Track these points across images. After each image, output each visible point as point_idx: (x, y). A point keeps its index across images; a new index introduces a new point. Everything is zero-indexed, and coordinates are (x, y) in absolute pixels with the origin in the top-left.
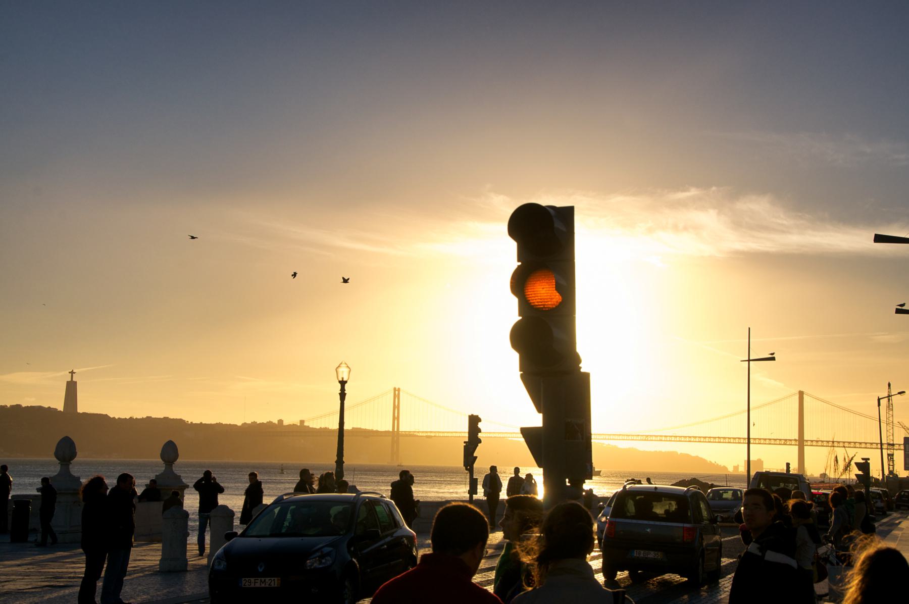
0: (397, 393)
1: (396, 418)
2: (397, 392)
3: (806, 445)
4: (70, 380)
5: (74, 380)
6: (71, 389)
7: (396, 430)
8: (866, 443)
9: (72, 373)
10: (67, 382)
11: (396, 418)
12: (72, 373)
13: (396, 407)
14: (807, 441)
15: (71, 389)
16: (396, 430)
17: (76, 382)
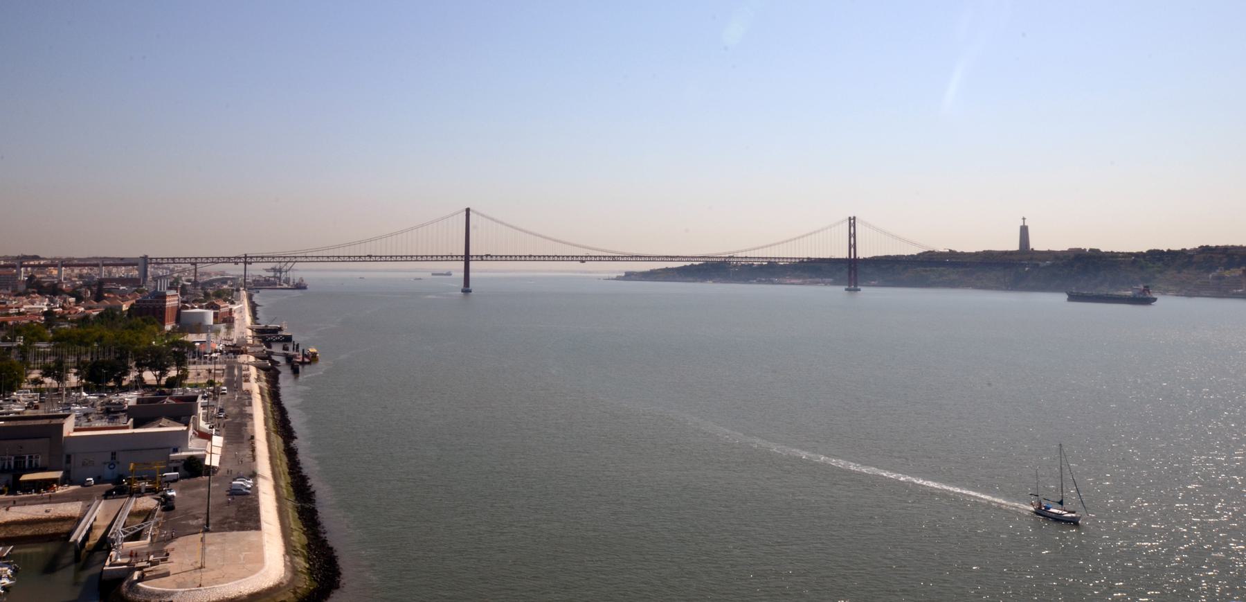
0: (852, 222)
1: (852, 246)
2: (852, 221)
6: (1024, 231)
7: (852, 257)
8: (427, 256)
9: (1024, 219)
11: (852, 246)
12: (1024, 219)
13: (852, 235)
14: (472, 256)
15: (1024, 231)
16: (852, 257)
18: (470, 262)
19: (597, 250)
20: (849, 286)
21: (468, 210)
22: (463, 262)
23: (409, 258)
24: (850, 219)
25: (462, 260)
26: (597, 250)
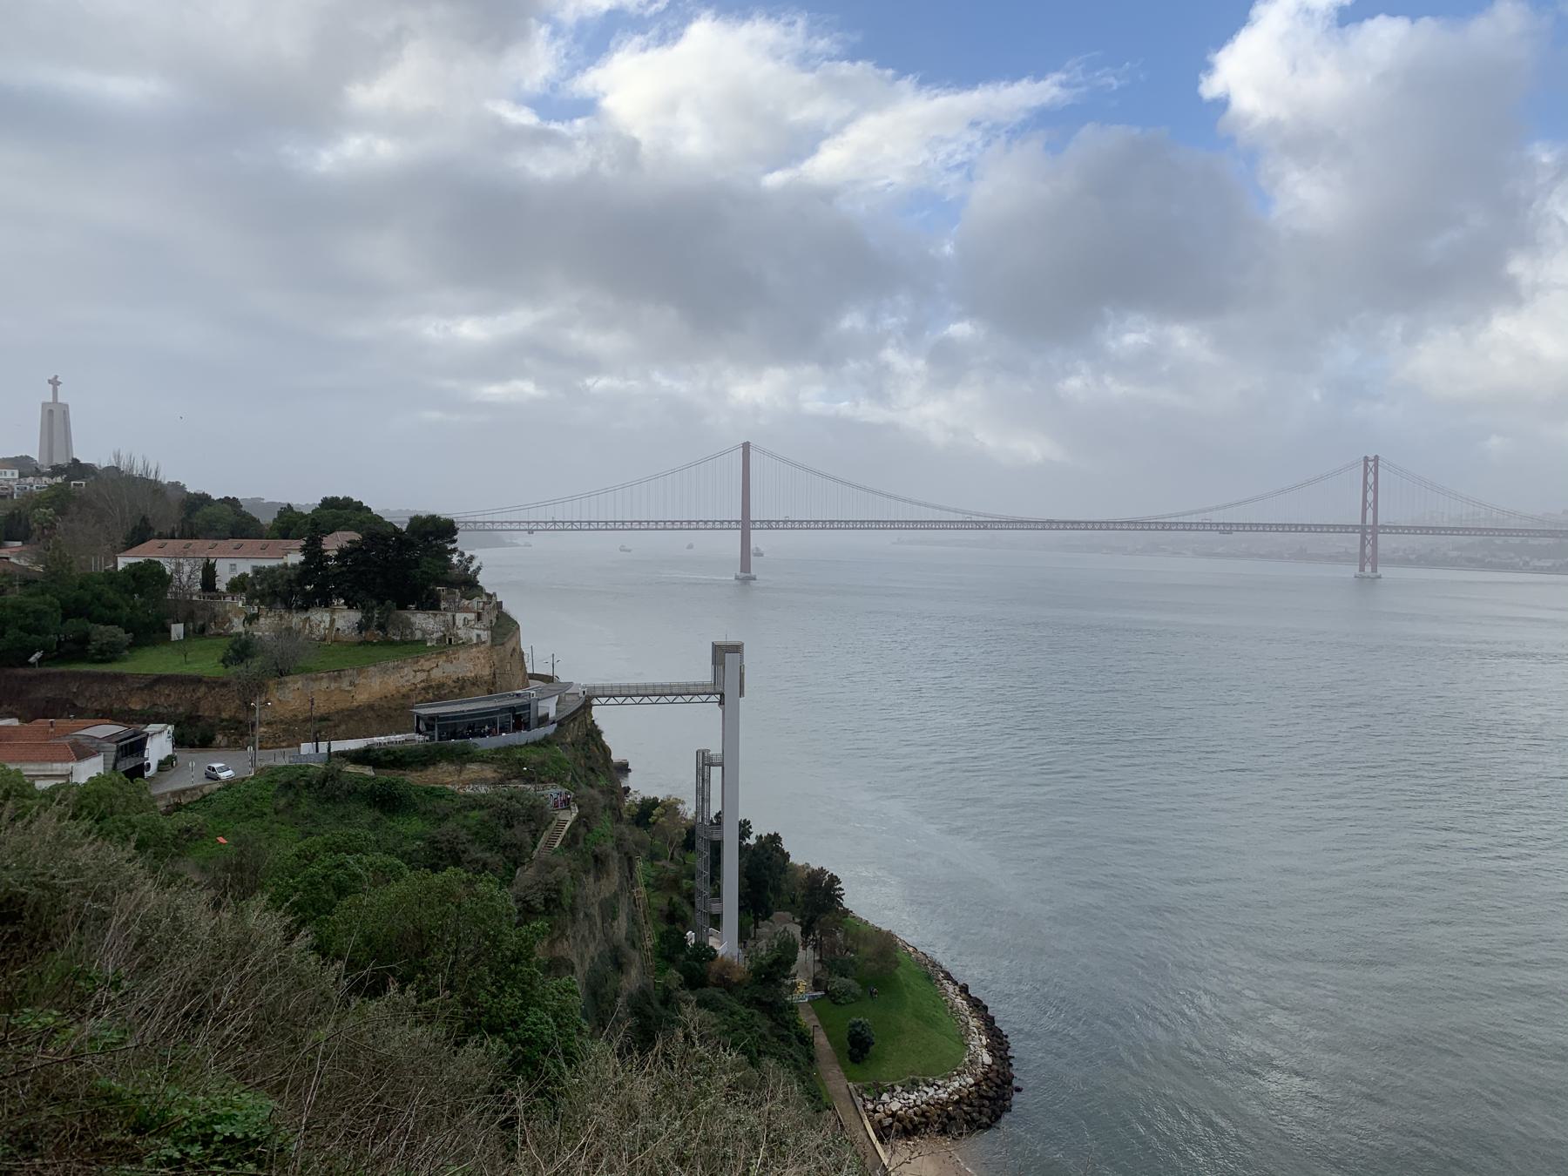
0: (1371, 465)
2: (1371, 464)
3: (754, 529)
7: (1369, 521)
16: (1369, 521)
18: (752, 531)
19: (956, 511)
21: (746, 447)
22: (740, 531)
23: (652, 525)
24: (1366, 457)
25: (739, 529)
26: (956, 511)
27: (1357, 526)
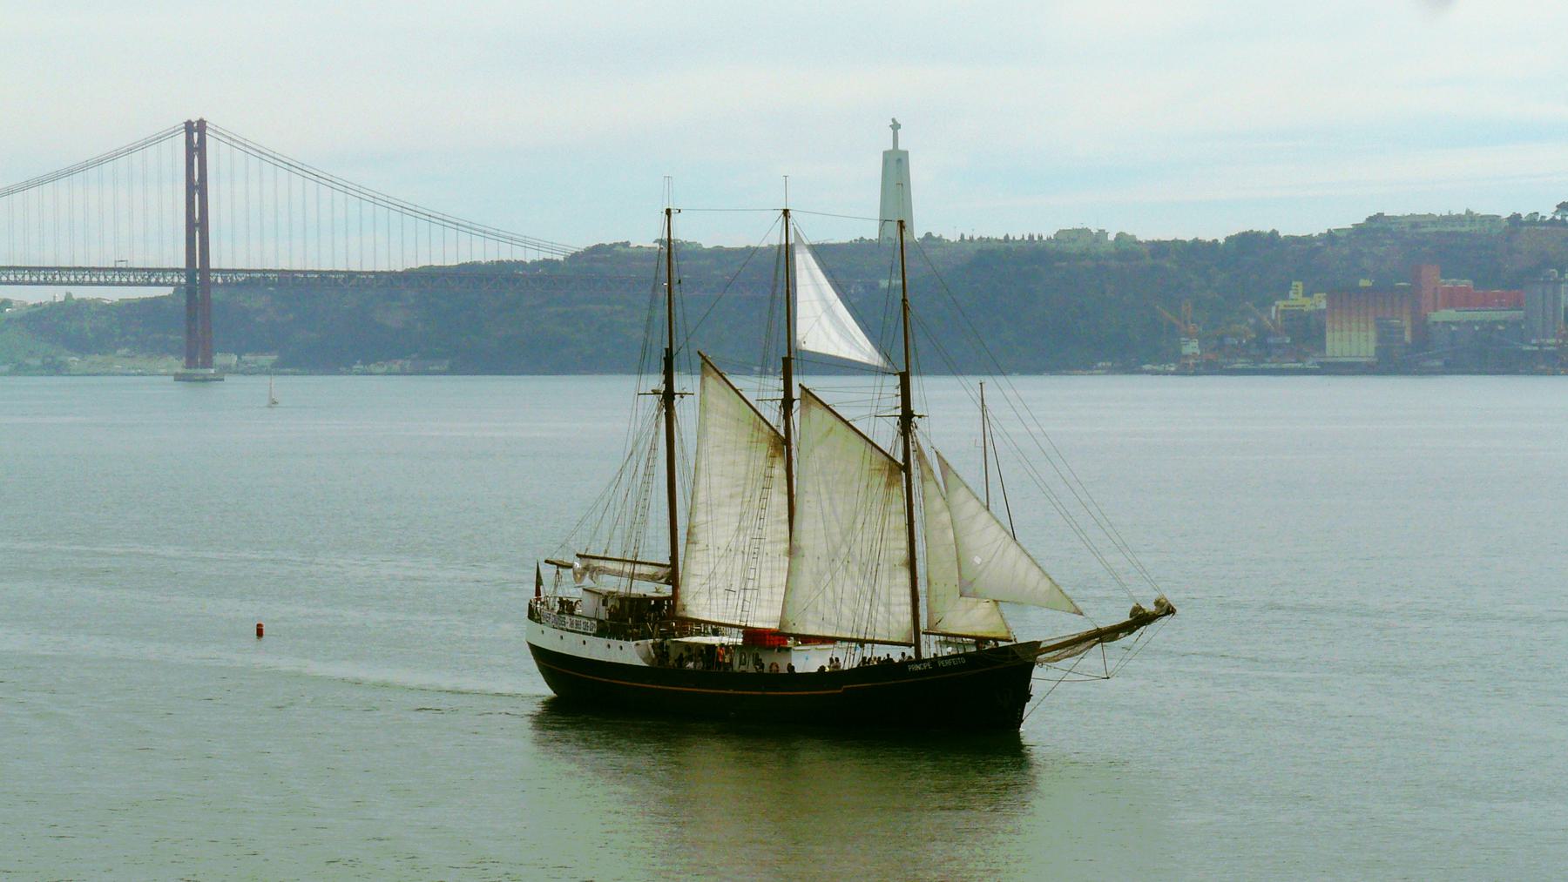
0: (196, 135)
1: (197, 226)
2: (196, 135)
4: (891, 148)
5: (901, 147)
6: (896, 166)
7: (198, 267)
9: (896, 126)
10: (885, 153)
11: (197, 226)
12: (896, 126)
13: (196, 188)
15: (896, 166)
16: (198, 267)
17: (906, 153)
20: (191, 363)
24: (189, 127)
27: (177, 270)
